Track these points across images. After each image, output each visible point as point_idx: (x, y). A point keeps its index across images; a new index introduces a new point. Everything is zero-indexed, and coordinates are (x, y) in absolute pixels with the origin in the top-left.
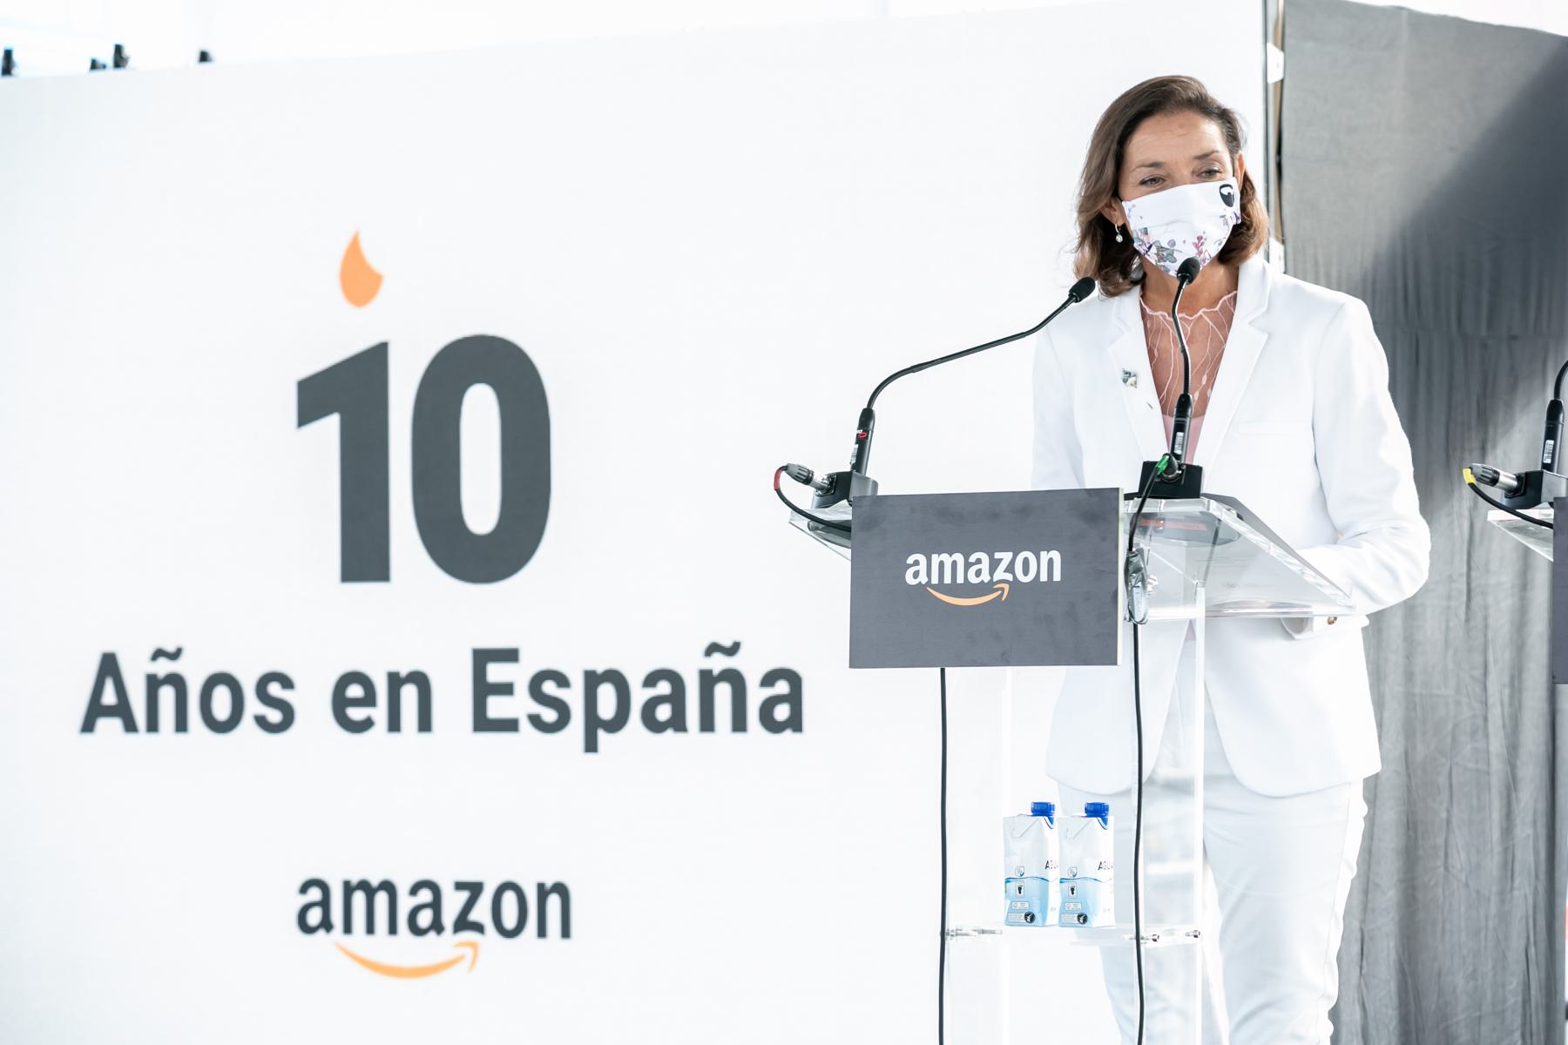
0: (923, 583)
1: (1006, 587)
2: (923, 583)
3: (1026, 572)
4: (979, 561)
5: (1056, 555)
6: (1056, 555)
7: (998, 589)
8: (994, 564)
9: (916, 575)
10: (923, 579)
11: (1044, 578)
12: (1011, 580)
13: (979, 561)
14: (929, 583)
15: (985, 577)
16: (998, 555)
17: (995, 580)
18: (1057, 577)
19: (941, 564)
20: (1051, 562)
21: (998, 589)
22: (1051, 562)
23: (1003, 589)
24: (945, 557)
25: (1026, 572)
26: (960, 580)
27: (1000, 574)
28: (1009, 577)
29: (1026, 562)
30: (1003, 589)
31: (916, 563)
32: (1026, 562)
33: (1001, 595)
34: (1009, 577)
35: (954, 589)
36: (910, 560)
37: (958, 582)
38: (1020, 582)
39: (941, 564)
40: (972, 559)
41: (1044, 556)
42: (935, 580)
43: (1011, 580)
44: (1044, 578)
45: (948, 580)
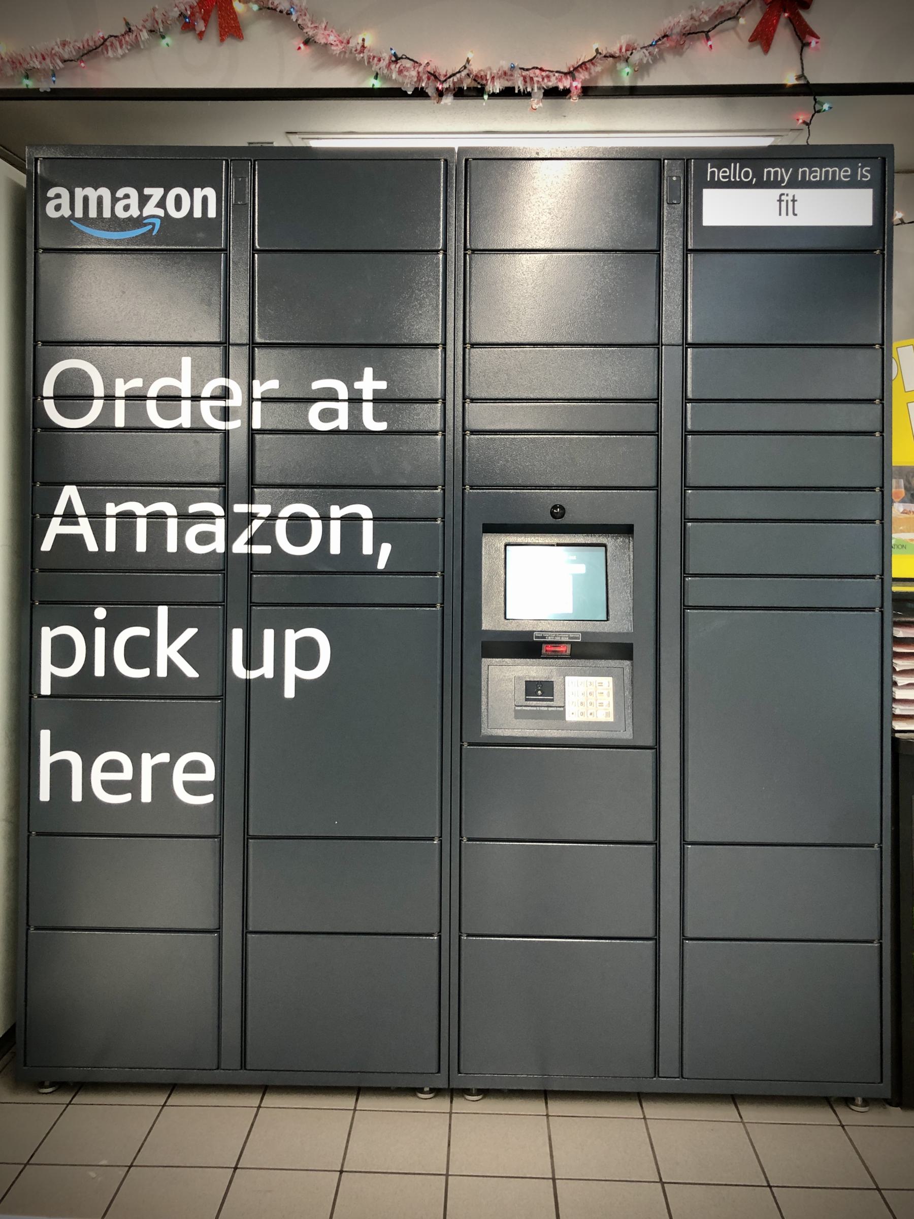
0: (66, 216)
1: (158, 222)
2: (66, 216)
3: (178, 206)
4: (127, 196)
5: (210, 193)
6: (210, 193)
7: (150, 224)
8: (144, 200)
9: (58, 208)
10: (66, 212)
11: (198, 214)
12: (163, 215)
13: (127, 196)
14: (72, 216)
15: (134, 212)
16: (147, 191)
17: (145, 215)
18: (212, 213)
19: (86, 200)
20: (205, 200)
21: (146, 225)
22: (205, 200)
23: (154, 225)
24: (89, 191)
25: (178, 206)
26: (107, 214)
27: (151, 209)
28: (161, 212)
29: (178, 199)
30: (154, 225)
31: (58, 196)
32: (178, 199)
33: (153, 229)
34: (161, 212)
35: (100, 222)
36: (51, 193)
37: (105, 216)
38: (215, 191)
39: (86, 200)
40: (120, 193)
41: (198, 193)
42: (79, 213)
43: (163, 215)
44: (198, 214)
45: (93, 213)
